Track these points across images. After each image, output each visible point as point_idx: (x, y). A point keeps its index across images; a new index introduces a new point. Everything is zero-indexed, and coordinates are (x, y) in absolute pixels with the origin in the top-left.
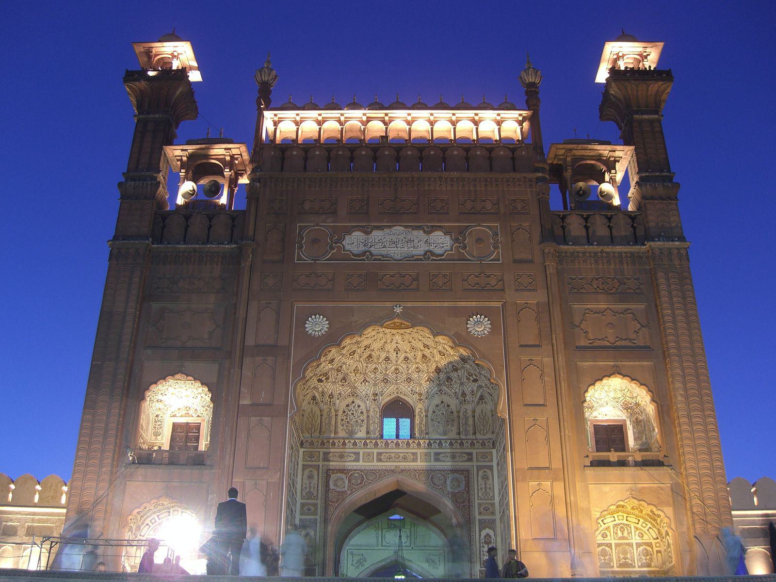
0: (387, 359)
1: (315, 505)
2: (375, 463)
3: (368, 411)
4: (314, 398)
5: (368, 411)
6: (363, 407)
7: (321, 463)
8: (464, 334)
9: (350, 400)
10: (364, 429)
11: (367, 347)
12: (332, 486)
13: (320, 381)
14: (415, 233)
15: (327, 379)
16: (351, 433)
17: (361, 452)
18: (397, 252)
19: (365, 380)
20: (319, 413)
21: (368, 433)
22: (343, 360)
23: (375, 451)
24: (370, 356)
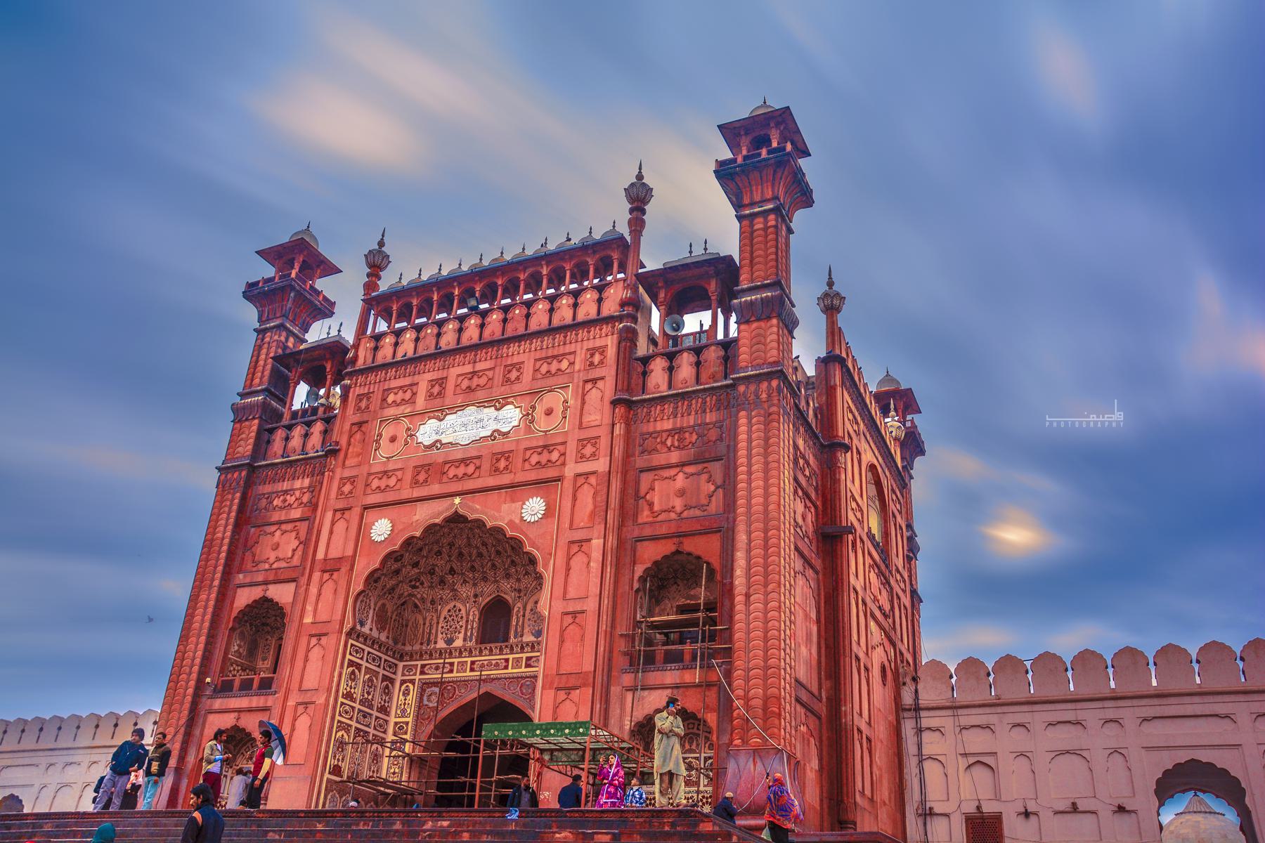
0: (480, 555)
1: (407, 723)
2: (468, 673)
3: (468, 615)
4: (416, 606)
5: (468, 615)
6: (463, 612)
7: (418, 677)
8: (517, 521)
9: (451, 605)
10: (461, 636)
11: (451, 545)
12: (425, 702)
13: (414, 587)
14: (486, 410)
15: (422, 584)
16: (449, 641)
17: (456, 661)
18: (464, 437)
19: (465, 582)
20: (421, 622)
21: (465, 640)
22: (431, 561)
23: (469, 660)
24: (461, 554)
